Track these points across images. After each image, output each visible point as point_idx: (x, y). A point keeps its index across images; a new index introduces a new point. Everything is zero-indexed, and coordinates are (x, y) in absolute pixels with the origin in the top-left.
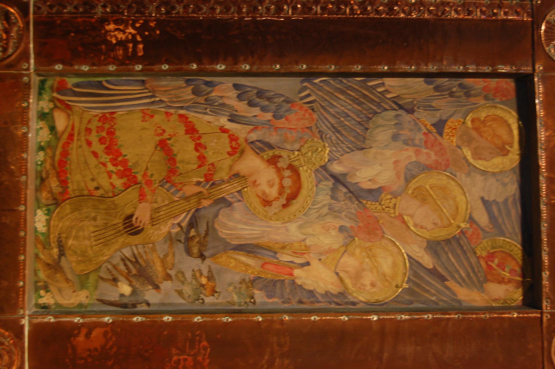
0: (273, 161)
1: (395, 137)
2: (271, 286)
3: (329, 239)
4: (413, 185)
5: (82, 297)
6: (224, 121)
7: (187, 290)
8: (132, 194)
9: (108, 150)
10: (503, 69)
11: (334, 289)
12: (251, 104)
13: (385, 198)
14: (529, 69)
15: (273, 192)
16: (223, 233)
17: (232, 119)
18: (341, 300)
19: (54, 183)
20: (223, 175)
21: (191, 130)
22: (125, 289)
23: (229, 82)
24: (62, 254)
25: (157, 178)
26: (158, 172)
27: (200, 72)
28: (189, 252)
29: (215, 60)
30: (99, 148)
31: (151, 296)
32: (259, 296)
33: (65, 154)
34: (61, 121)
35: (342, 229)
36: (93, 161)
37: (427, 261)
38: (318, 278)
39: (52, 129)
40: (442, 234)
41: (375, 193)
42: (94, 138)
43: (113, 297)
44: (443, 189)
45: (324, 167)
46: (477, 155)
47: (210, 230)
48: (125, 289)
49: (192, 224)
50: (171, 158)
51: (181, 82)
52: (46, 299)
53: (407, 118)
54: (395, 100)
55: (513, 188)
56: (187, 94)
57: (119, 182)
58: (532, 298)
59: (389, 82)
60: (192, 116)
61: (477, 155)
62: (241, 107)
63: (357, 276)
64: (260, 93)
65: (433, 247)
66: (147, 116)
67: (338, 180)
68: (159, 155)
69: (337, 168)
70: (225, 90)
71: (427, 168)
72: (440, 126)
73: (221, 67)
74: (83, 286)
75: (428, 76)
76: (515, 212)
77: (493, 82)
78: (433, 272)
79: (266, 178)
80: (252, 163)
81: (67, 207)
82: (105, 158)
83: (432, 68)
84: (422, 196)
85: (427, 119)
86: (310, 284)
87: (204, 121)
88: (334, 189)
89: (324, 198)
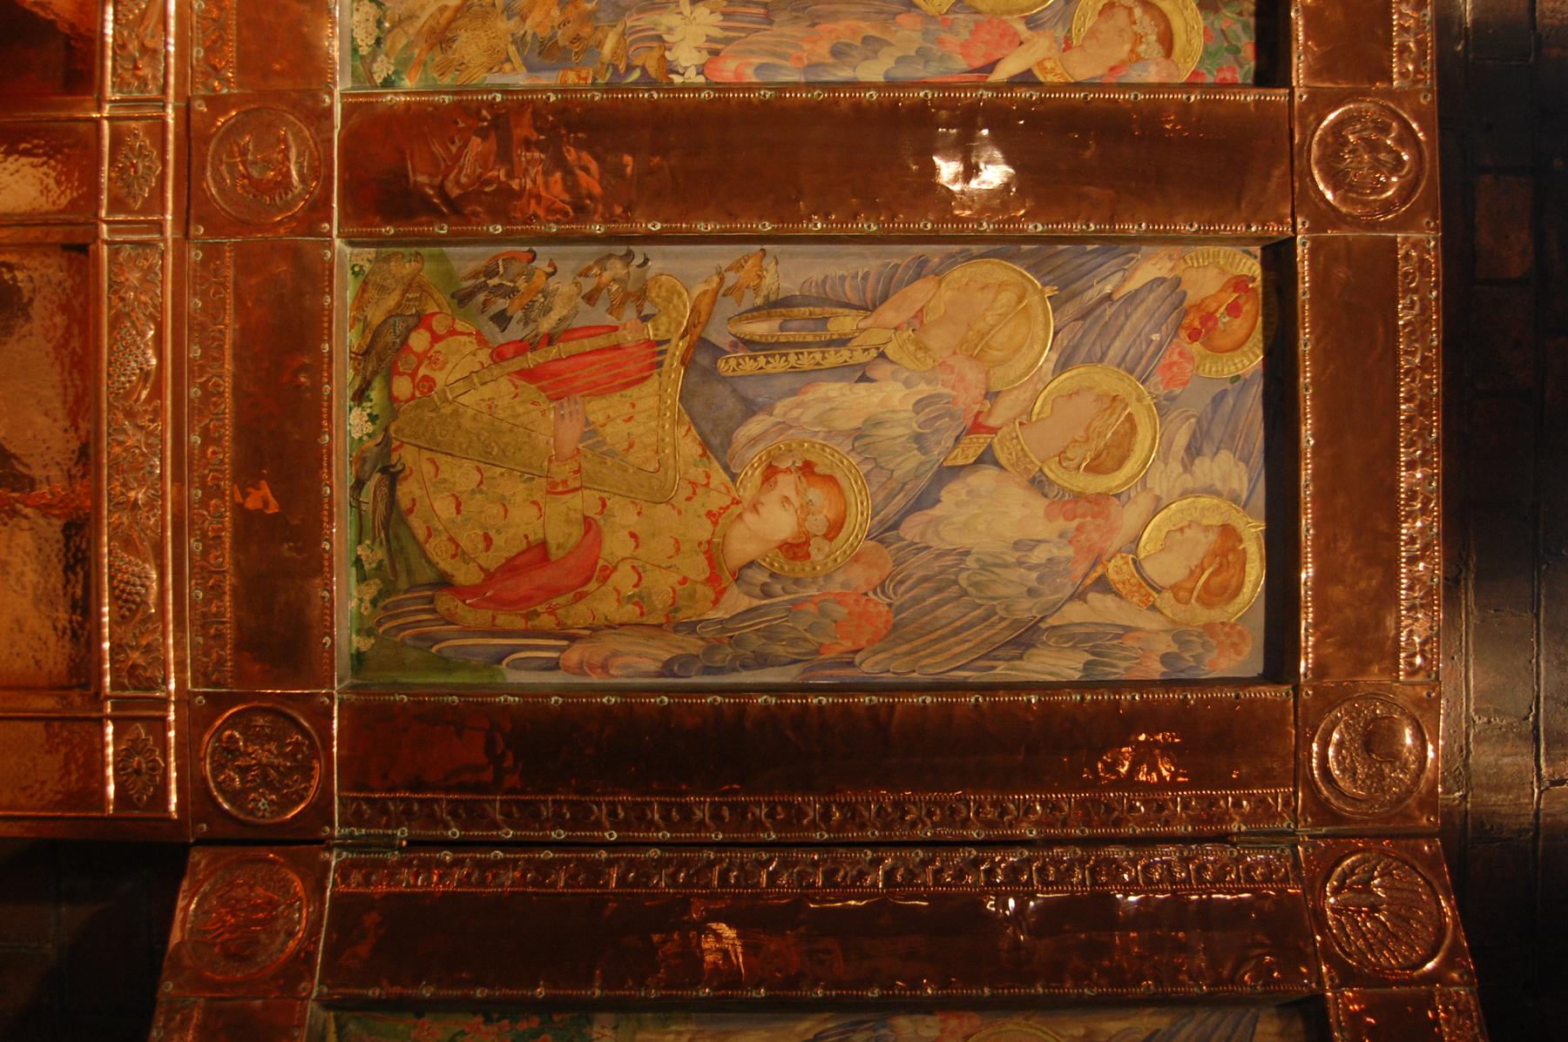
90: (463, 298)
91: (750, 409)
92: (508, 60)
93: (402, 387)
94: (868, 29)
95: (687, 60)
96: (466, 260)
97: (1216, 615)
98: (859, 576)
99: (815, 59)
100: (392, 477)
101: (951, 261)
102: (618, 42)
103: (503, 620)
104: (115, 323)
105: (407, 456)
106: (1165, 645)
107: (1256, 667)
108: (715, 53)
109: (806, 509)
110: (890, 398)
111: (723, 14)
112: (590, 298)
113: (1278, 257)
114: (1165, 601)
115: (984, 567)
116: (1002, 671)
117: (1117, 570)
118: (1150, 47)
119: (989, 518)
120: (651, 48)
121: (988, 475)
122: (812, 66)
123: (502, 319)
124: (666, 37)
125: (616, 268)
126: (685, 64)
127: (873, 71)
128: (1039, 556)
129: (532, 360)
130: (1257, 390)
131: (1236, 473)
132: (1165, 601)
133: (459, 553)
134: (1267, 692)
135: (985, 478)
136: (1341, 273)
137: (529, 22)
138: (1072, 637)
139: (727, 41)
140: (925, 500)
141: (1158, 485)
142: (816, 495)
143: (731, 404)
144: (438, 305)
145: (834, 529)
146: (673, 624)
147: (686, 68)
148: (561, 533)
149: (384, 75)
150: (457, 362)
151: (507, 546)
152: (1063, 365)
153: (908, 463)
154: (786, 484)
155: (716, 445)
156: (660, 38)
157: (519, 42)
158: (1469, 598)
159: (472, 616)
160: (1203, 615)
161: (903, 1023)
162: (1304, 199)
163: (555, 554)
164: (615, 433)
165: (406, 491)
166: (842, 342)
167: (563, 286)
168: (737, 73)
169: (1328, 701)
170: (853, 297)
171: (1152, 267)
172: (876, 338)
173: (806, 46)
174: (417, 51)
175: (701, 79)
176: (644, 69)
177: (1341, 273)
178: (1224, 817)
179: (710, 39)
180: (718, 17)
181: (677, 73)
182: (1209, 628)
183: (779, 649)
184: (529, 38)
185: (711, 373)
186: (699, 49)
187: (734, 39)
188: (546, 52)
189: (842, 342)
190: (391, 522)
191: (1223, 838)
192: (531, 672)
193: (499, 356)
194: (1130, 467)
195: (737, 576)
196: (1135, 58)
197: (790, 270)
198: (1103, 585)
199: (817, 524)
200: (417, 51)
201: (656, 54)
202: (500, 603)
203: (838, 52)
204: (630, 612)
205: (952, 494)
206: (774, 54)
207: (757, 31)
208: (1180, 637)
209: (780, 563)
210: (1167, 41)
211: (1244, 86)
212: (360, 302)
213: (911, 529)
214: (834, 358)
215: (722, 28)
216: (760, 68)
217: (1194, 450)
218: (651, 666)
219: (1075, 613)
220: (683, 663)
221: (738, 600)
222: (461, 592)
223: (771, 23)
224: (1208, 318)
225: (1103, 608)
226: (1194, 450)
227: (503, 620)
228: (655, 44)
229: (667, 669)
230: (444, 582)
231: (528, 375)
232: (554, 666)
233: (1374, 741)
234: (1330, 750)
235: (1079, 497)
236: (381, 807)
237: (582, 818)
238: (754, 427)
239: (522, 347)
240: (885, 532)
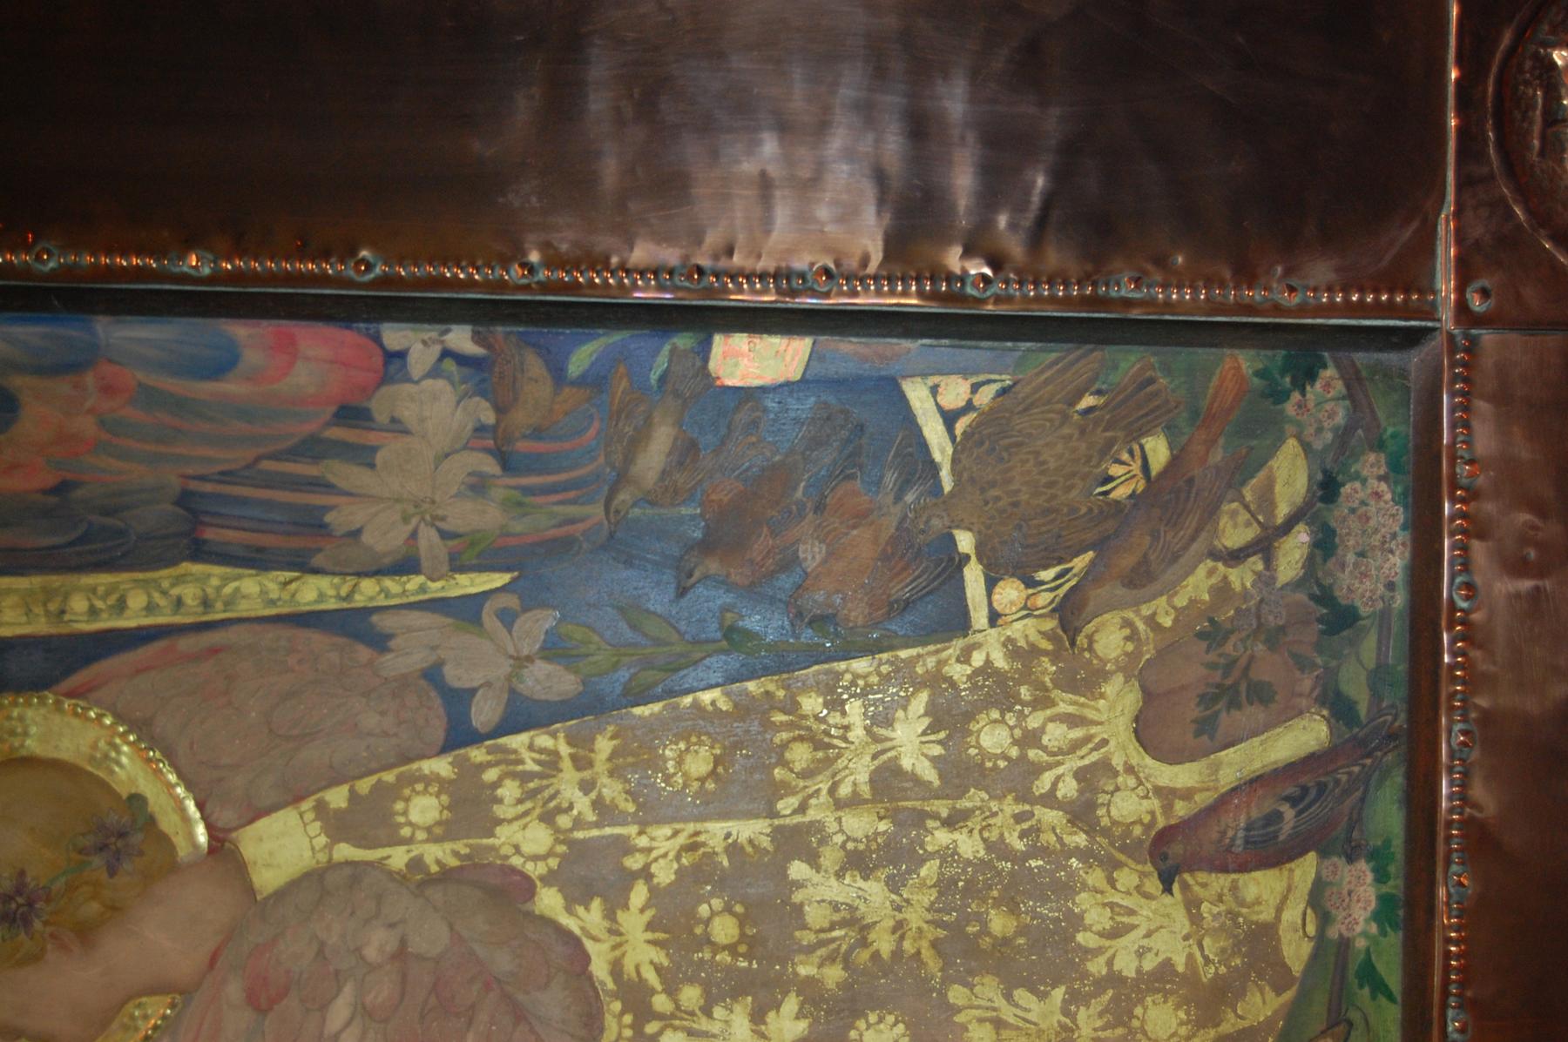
92: (949, 418)
99: (63, 386)
102: (629, 459)
108: (352, 413)
111: (321, 529)
120: (537, 433)
122: (69, 367)
124: (490, 466)
126: (440, 384)
137: (889, 525)
139: (313, 448)
147: (434, 373)
149: (1315, 391)
156: (507, 463)
157: (919, 462)
168: (287, 346)
173: (86, 426)
174: (1217, 456)
175: (395, 335)
176: (558, 373)
179: (364, 456)
180: (342, 517)
181: (462, 360)
184: (890, 478)
186: (398, 427)
187: (293, 453)
200: (1217, 456)
201: (521, 418)
206: (180, 405)
207: (227, 476)
215: (328, 487)
216: (222, 365)
223: (185, 499)
228: (522, 446)
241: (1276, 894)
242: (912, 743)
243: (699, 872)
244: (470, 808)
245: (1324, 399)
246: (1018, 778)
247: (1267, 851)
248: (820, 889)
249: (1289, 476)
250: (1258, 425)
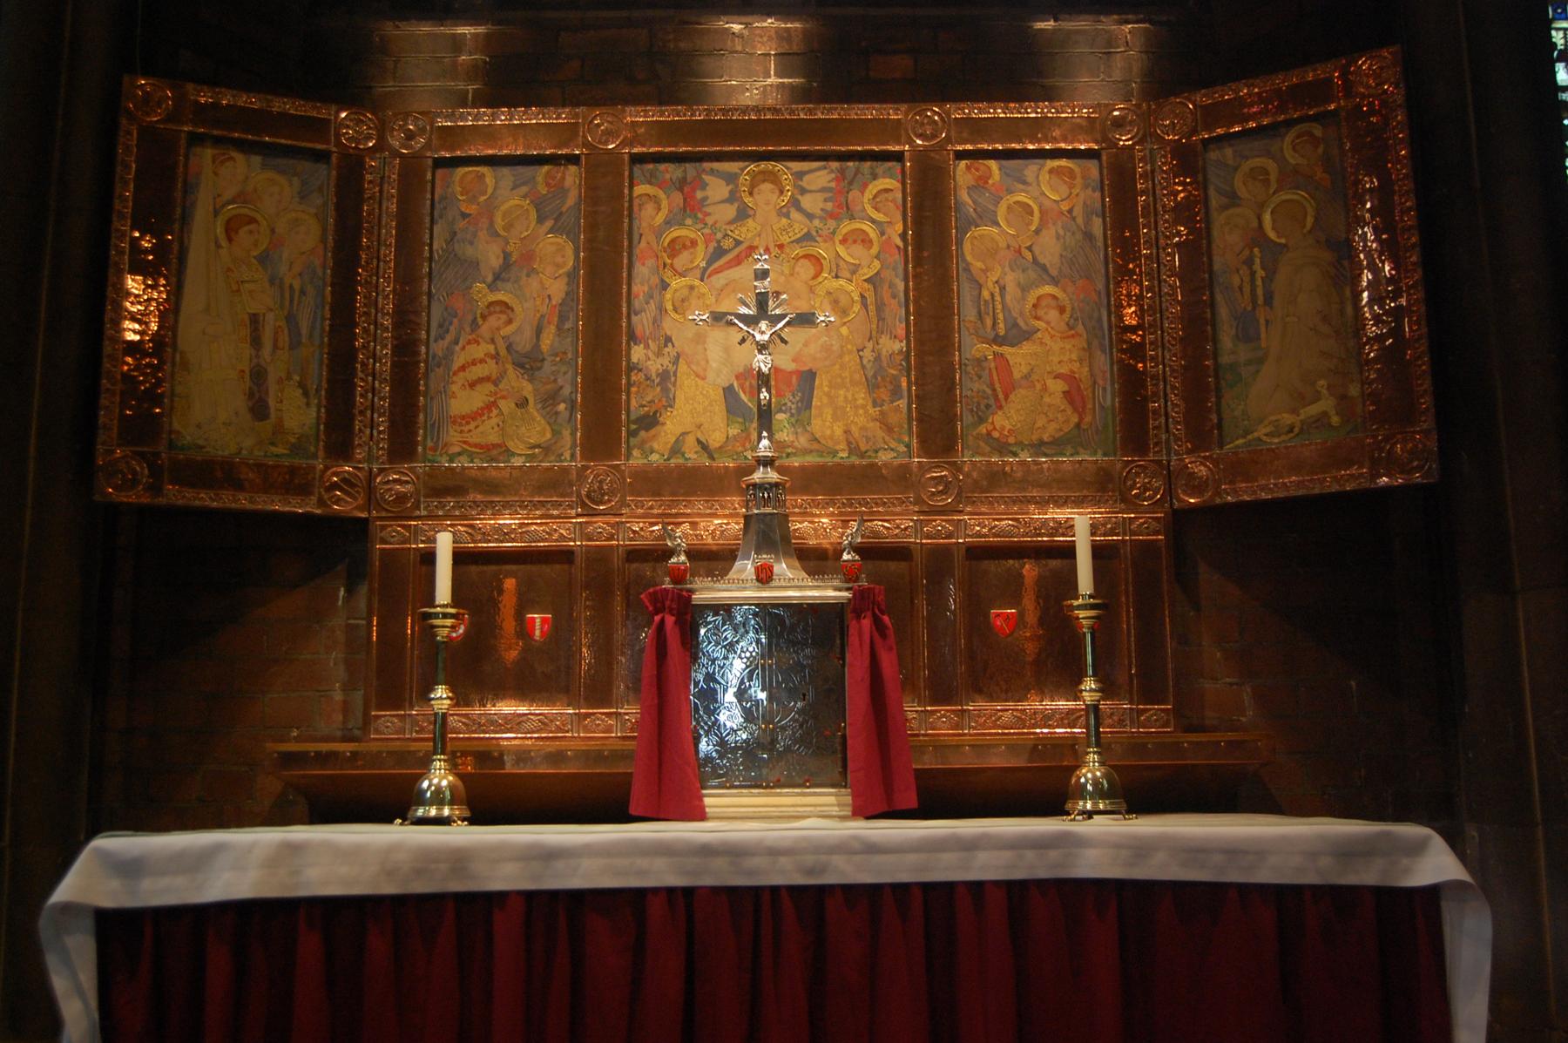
0: (484, 317)
1: (471, 243)
2: (562, 318)
3: (534, 283)
4: (502, 233)
5: (566, 433)
6: (457, 348)
7: (563, 369)
8: (502, 404)
9: (474, 419)
10: (429, 176)
11: (565, 280)
12: (448, 331)
13: (509, 249)
14: (430, 162)
15: (504, 317)
16: (528, 347)
17: (457, 343)
18: (572, 276)
19: (494, 452)
20: (491, 348)
21: (463, 368)
22: (562, 407)
23: (433, 345)
24: (538, 446)
25: (493, 388)
26: (490, 387)
27: (426, 362)
28: (539, 369)
29: (418, 353)
30: (472, 426)
31: (567, 391)
32: (568, 326)
33: (476, 446)
34: (456, 449)
35: (528, 276)
36: (481, 429)
37: (549, 224)
38: (558, 289)
39: (459, 454)
40: (533, 215)
41: (506, 256)
42: (466, 428)
43: (566, 414)
44: (504, 215)
45: (489, 286)
46: (484, 193)
47: (526, 356)
48: (562, 407)
49: (522, 366)
50: (481, 380)
51: (432, 375)
52: (567, 455)
53: (459, 236)
54: (448, 243)
55: (505, 171)
56: (440, 371)
57: (495, 412)
58: (573, 160)
59: (435, 247)
60: (456, 366)
61: (484, 193)
62: (449, 338)
63: (558, 266)
64: (441, 326)
65: (541, 220)
66: (454, 395)
67: (497, 277)
68: (479, 387)
69: (490, 278)
70: (438, 348)
71: (492, 223)
72: (464, 216)
73: (423, 349)
74: (560, 433)
75: (432, 222)
76: (520, 169)
77: (438, 182)
78: (556, 220)
79: (493, 321)
80: (485, 329)
81: (511, 445)
82: (479, 421)
83: (427, 220)
84: (509, 227)
85: (462, 224)
86: (563, 295)
87: (459, 360)
88: (503, 280)
89: (509, 286)
90: (982, 420)
91: (1016, 325)
93: (1011, 440)
94: (886, 287)
95: (899, 346)
96: (968, 418)
97: (1079, 176)
98: (1070, 289)
100: (1042, 443)
101: (964, 260)
103: (1090, 406)
104: (995, 535)
105: (1035, 437)
106: (1089, 191)
107: (1095, 162)
109: (1048, 306)
110: (1011, 280)
112: (980, 377)
113: (960, 155)
114: (1075, 191)
115: (1065, 249)
116: (1100, 243)
117: (1065, 207)
118: (890, 196)
119: (1050, 248)
121: (1035, 248)
123: (988, 406)
125: (969, 368)
127: (901, 286)
128: (1061, 232)
129: (1001, 396)
130: (1004, 162)
131: (1031, 169)
132: (1075, 191)
133: (1067, 421)
134: (1104, 158)
135: (1036, 249)
136: (965, 135)
138: (1088, 222)
140: (1044, 268)
141: (1037, 194)
142: (1044, 303)
143: (1014, 331)
144: (983, 429)
145: (1054, 297)
146: (1089, 349)
148: (1058, 387)
150: (1003, 421)
151: (1064, 405)
152: (997, 224)
153: (1032, 274)
154: (1040, 313)
155: (1027, 335)
158: (1048, 82)
159: (1088, 419)
160: (1079, 180)
161: (1216, 267)
162: (941, 147)
163: (1066, 388)
164: (1025, 370)
165: (1046, 438)
166: (992, 295)
167: (976, 386)
169: (1105, 139)
170: (975, 293)
171: (964, 196)
172: (990, 284)
177: (965, 135)
178: (1145, 172)
182: (1083, 177)
183: (1096, 315)
185: (1004, 338)
188: (896, 393)
189: (992, 295)
190: (1058, 444)
191: (1153, 171)
192: (1108, 396)
193: (1000, 407)
194: (1031, 203)
195: (1071, 328)
196: (894, 201)
197: (969, 313)
198: (1070, 211)
199: (1053, 303)
202: (1084, 407)
203: (894, 296)
204: (1086, 364)
205: (1042, 260)
208: (1086, 187)
209: (1067, 316)
210: (887, 191)
211: (904, 166)
212: (983, 455)
213: (1054, 273)
214: (998, 298)
217: (1024, 183)
218: (1103, 358)
219: (1080, 220)
220: (1101, 346)
221: (1080, 328)
222: (1081, 419)
224: (980, 178)
225: (1078, 211)
226: (1024, 183)
227: (1090, 406)
229: (1104, 351)
230: (1078, 425)
231: (1006, 397)
232: (1104, 389)
233: (1119, 124)
234: (1125, 140)
235: (1041, 219)
236: (1156, 444)
237: (1155, 377)
238: (1022, 324)
239: (997, 399)
240: (1055, 281)
241: (843, 446)
242: (860, 402)
243: (843, 379)
244: (850, 352)
245: (902, 448)
246: (856, 415)
247: (849, 443)
248: (842, 392)
249: (893, 444)
250: (900, 441)
